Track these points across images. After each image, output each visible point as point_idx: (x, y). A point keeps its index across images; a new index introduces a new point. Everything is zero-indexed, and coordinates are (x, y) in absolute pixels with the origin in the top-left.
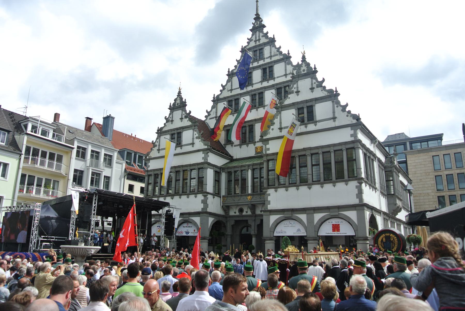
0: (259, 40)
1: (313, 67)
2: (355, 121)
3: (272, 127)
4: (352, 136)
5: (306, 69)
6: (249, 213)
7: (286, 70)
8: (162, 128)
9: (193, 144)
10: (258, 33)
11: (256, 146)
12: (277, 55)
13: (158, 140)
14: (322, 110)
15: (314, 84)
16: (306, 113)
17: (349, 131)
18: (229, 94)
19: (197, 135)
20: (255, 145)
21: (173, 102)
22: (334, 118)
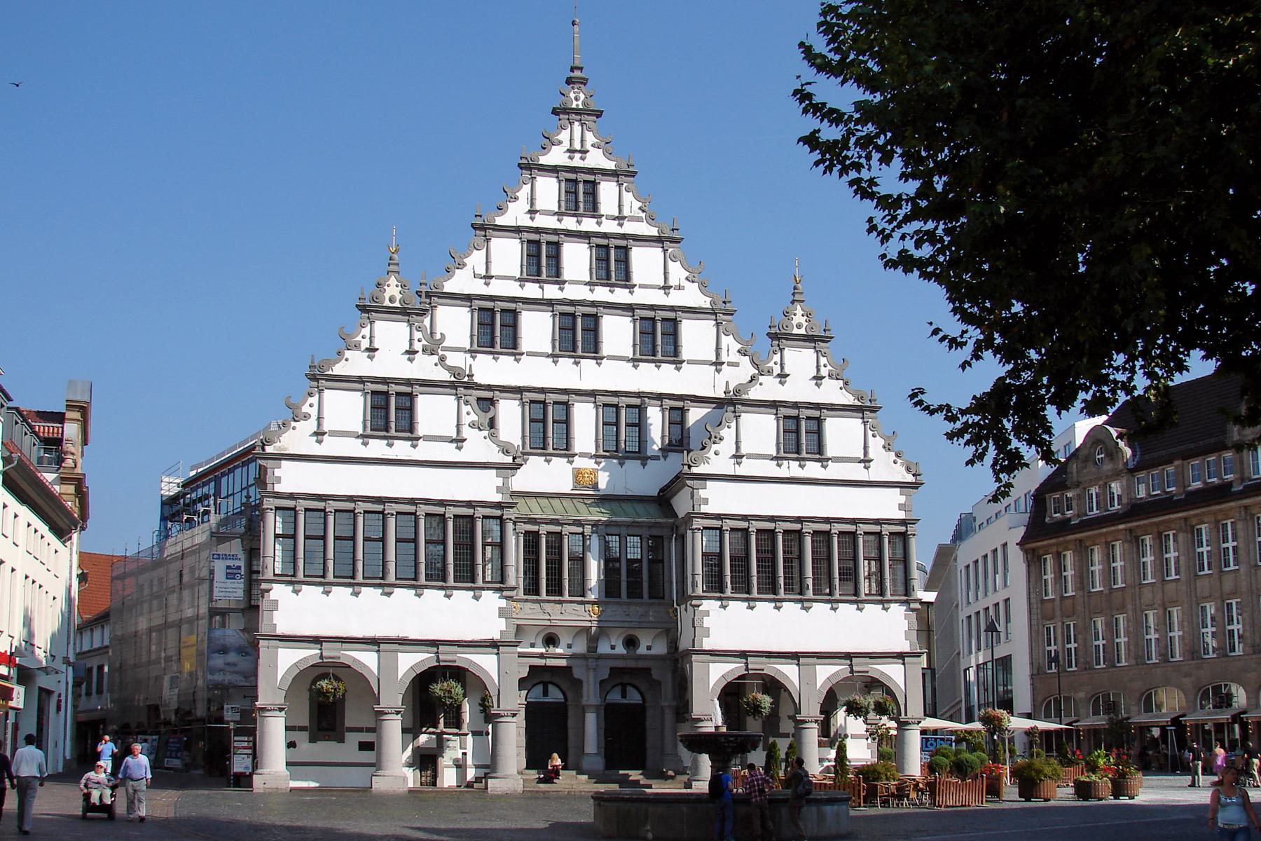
2: (910, 478)
3: (715, 447)
4: (901, 507)
5: (805, 324)
7: (666, 273)
9: (459, 441)
11: (574, 465)
12: (639, 220)
13: (314, 400)
17: (896, 496)
18: (478, 288)
19: (474, 417)
20: (571, 462)
22: (866, 461)
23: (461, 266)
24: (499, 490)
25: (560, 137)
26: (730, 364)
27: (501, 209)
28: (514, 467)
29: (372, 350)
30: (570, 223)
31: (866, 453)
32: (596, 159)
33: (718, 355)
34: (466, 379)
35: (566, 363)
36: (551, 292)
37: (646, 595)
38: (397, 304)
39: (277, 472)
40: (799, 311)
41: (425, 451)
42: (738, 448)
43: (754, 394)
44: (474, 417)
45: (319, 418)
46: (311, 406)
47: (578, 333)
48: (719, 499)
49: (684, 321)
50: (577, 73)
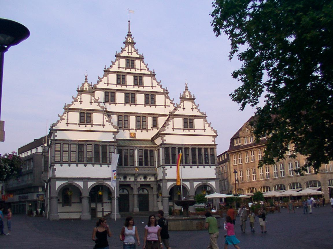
0: (131, 53)
1: (193, 96)
2: (215, 134)
3: (167, 126)
4: (213, 141)
5: (189, 95)
6: (132, 179)
8: (70, 105)
10: (130, 46)
12: (145, 70)
13: (66, 115)
14: (198, 123)
15: (193, 106)
16: (188, 122)
18: (106, 87)
19: (107, 119)
20: (129, 131)
21: (80, 86)
23: (101, 81)
24: (113, 138)
25: (125, 49)
26: (168, 106)
27: (111, 67)
28: (118, 132)
29: (81, 102)
30: (128, 70)
31: (204, 128)
32: (134, 55)
33: (165, 104)
34: (105, 109)
35: (128, 105)
36: (124, 88)
37: (149, 165)
38: (87, 90)
39: (56, 134)
40: (187, 92)
41: (95, 128)
42: (173, 127)
43: (177, 113)
44: (107, 119)
45: (68, 120)
46: (65, 116)
47: (130, 98)
48: (169, 140)
49: (157, 95)
50: (129, 34)
